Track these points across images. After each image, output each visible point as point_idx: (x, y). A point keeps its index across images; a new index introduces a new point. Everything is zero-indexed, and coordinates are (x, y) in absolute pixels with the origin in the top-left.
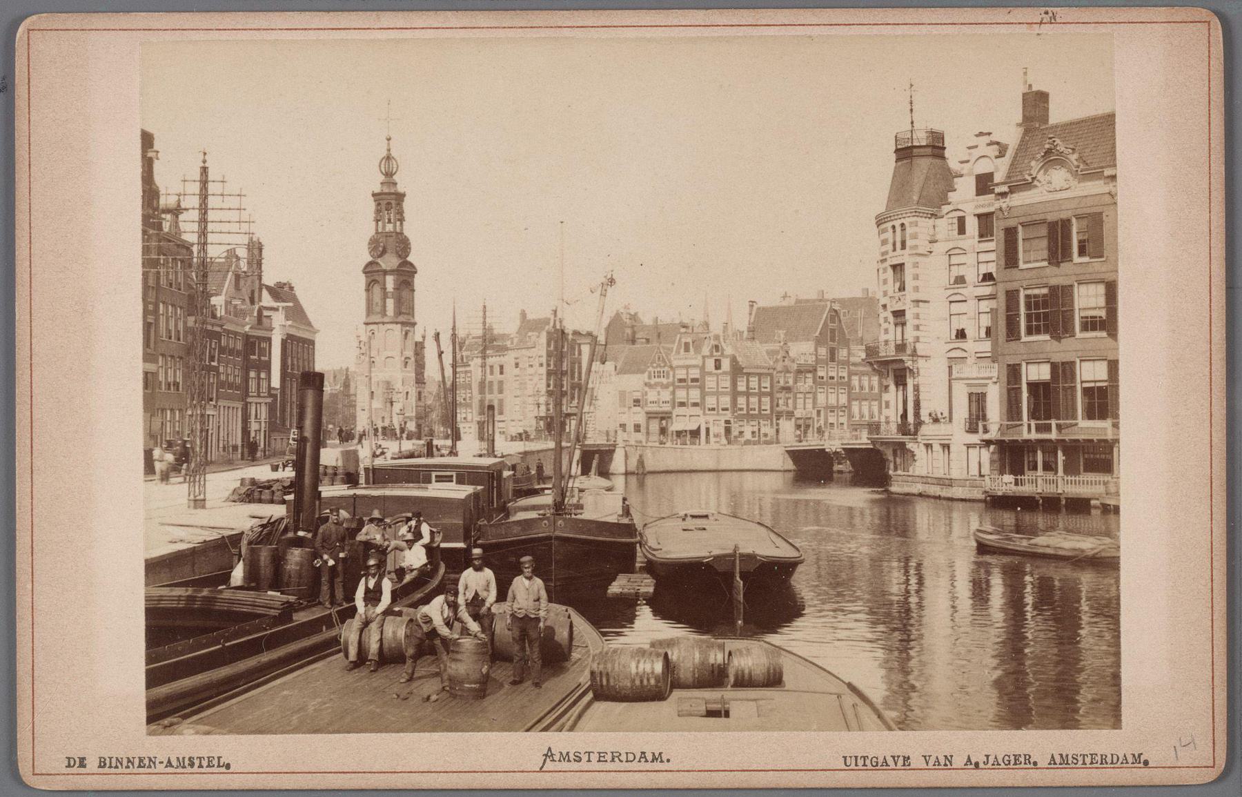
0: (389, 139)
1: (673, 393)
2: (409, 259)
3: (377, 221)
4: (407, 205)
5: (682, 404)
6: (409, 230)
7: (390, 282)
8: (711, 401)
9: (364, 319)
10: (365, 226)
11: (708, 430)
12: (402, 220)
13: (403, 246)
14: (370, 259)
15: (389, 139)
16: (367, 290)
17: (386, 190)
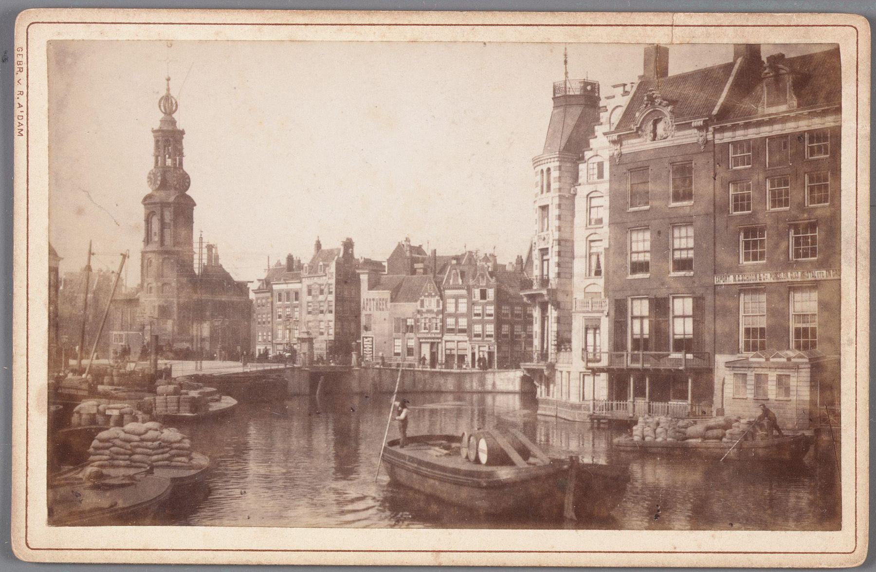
0: (168, 80)
1: (443, 321)
2: (188, 193)
4: (186, 142)
5: (451, 331)
6: (187, 167)
7: (168, 216)
8: (478, 329)
11: (473, 354)
12: (181, 154)
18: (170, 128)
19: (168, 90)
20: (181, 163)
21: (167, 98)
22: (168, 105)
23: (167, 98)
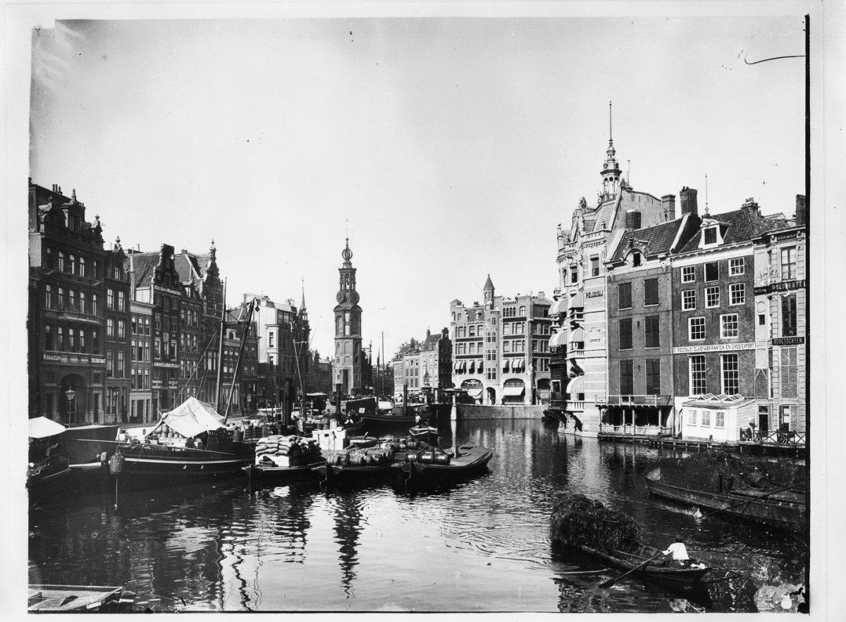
0: (347, 240)
3: (341, 284)
4: (357, 275)
7: (347, 316)
9: (334, 337)
10: (334, 285)
12: (354, 283)
13: (355, 297)
14: (338, 304)
15: (347, 240)
16: (336, 321)
17: (345, 267)
18: (349, 267)
19: (347, 245)
20: (354, 288)
21: (347, 250)
22: (347, 254)
23: (347, 250)
